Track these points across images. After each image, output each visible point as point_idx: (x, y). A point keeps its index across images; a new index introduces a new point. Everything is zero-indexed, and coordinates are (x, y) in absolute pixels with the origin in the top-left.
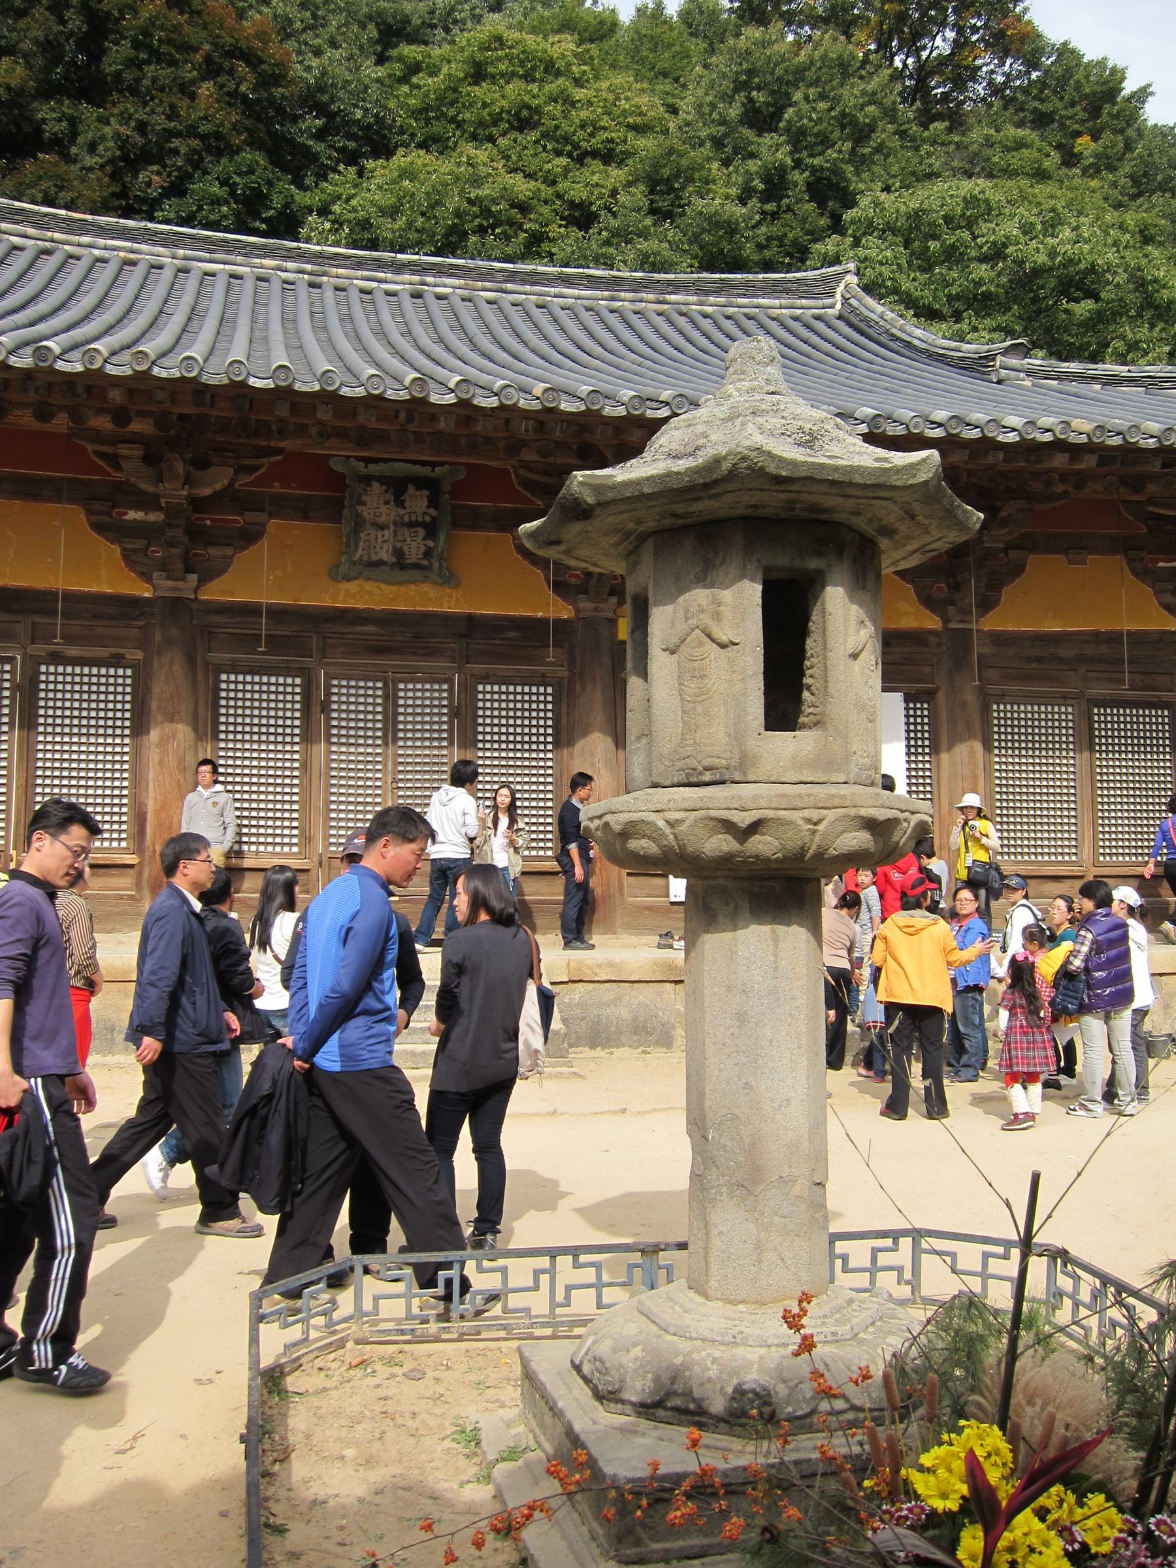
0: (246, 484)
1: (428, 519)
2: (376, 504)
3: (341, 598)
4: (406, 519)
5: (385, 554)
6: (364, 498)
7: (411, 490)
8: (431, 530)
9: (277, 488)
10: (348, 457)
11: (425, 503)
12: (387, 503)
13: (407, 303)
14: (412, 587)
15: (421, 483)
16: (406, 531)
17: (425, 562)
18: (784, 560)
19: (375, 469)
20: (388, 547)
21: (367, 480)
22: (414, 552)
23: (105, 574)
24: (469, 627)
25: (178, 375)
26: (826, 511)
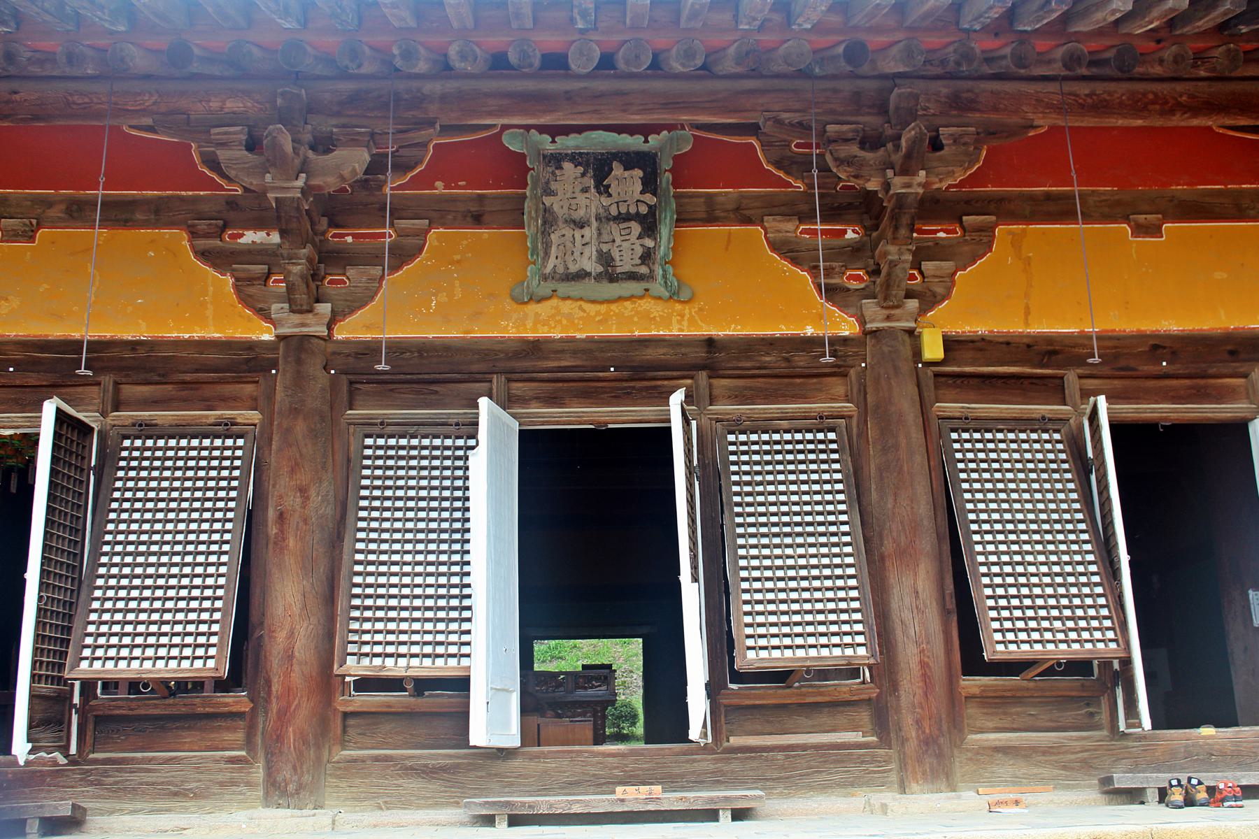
0: (400, 187)
1: (644, 210)
2: (570, 192)
3: (529, 325)
4: (614, 212)
6: (553, 186)
7: (618, 170)
8: (649, 225)
9: (440, 188)
10: (528, 128)
11: (639, 187)
12: (585, 190)
14: (628, 304)
15: (631, 160)
16: (615, 228)
17: (644, 270)
19: (569, 143)
20: (591, 251)
21: (556, 160)
22: (627, 257)
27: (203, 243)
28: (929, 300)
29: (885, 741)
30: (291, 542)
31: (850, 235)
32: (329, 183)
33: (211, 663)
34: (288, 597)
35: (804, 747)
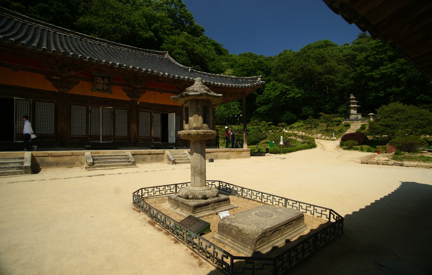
2: (99, 80)
5: (101, 88)
8: (109, 85)
13: (98, 46)
21: (98, 76)
23: (49, 87)
24: (114, 101)
28: (139, 97)
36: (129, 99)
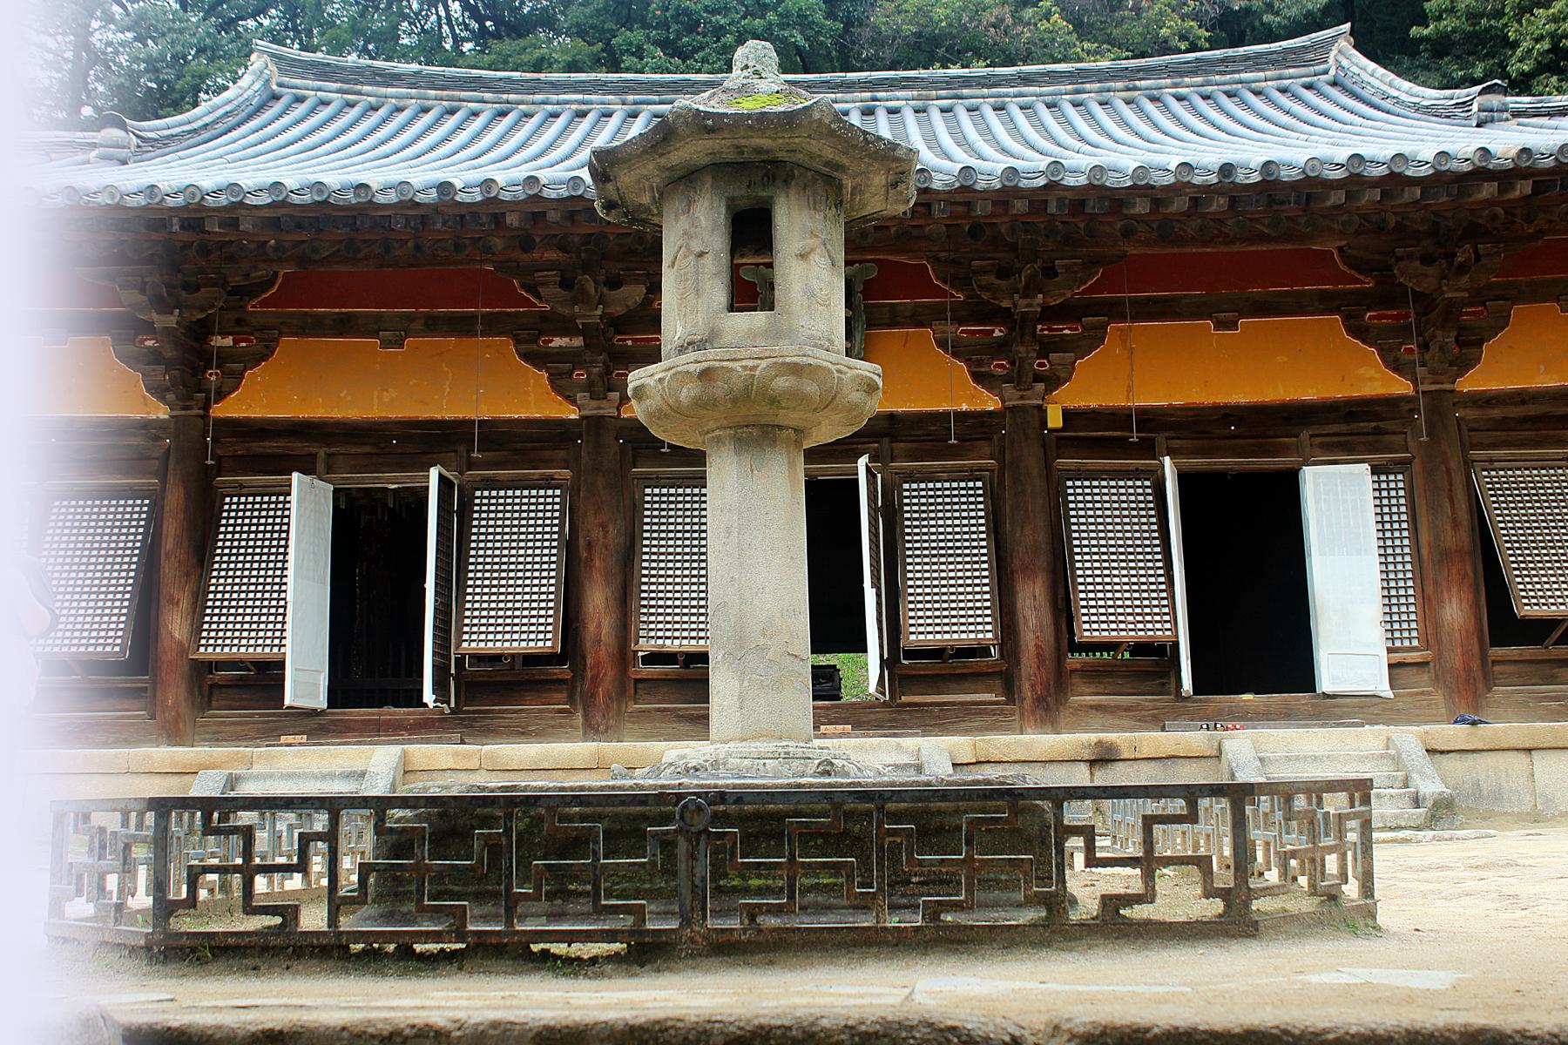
10: (757, 265)
18: (740, 191)
25: (566, 194)
26: (767, 152)
27: (524, 347)
28: (1053, 382)
29: (1011, 700)
30: (597, 563)
31: (997, 333)
32: (619, 310)
33: (549, 644)
34: (598, 600)
35: (953, 704)
36: (992, 404)
